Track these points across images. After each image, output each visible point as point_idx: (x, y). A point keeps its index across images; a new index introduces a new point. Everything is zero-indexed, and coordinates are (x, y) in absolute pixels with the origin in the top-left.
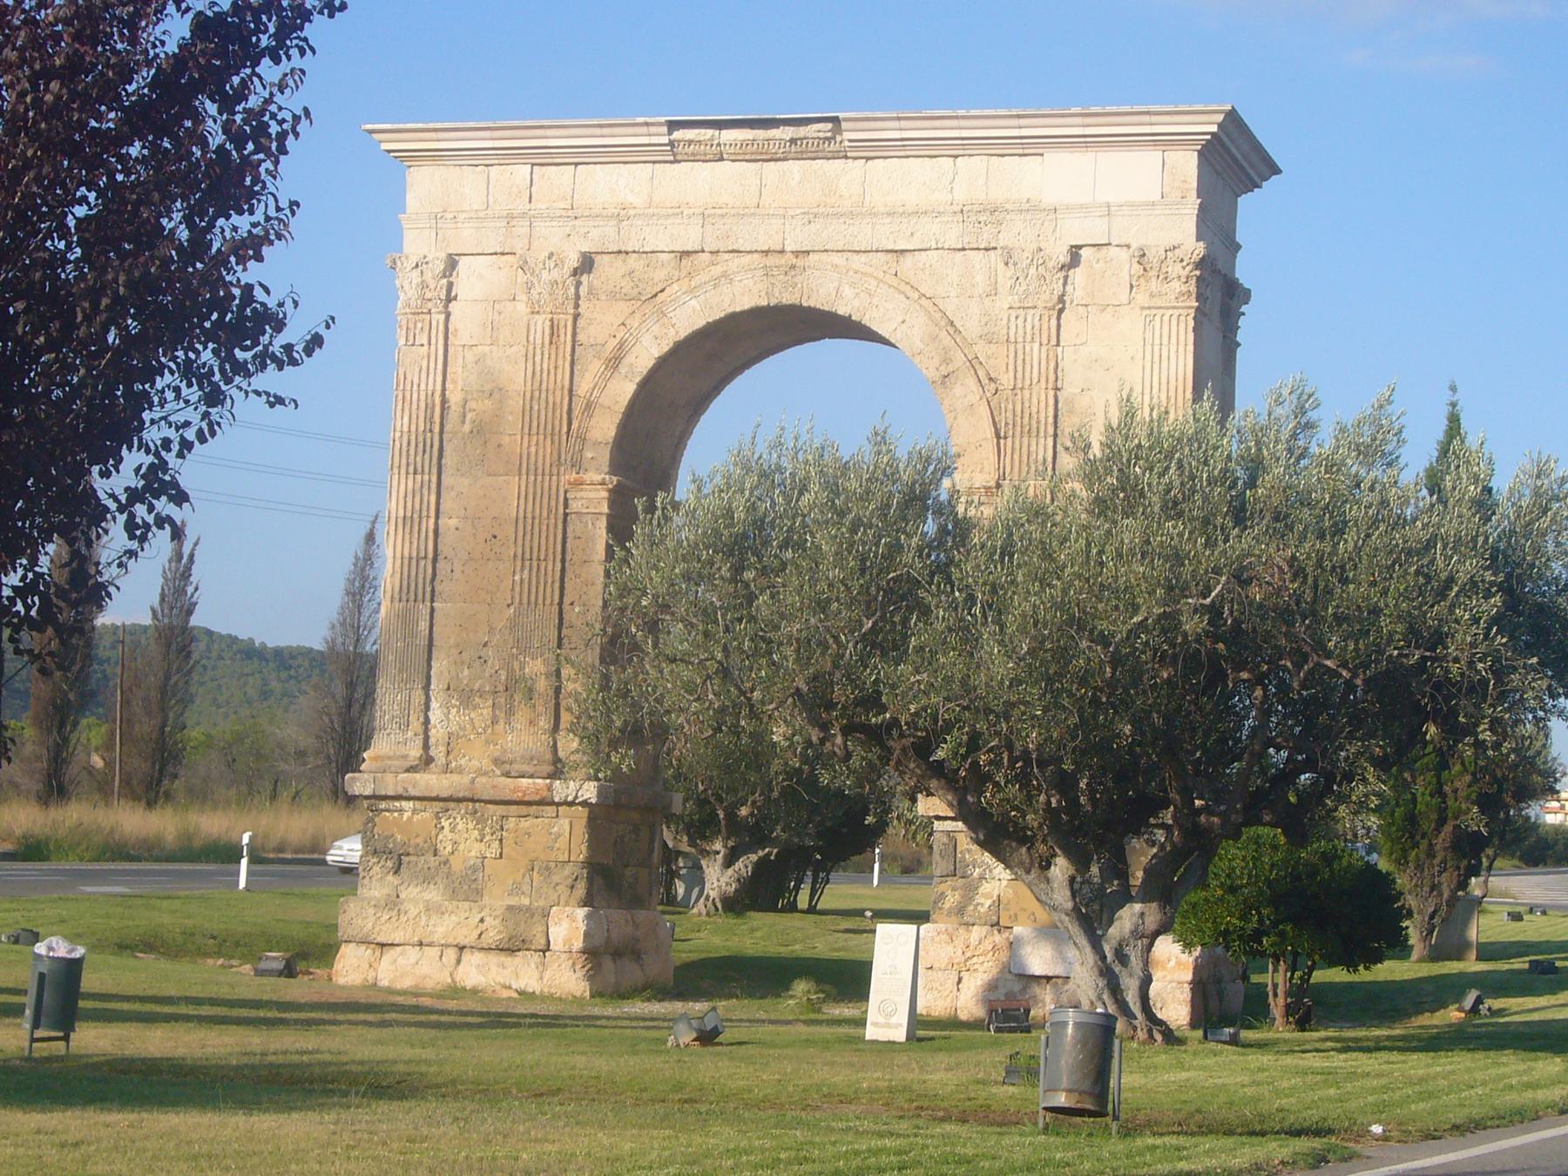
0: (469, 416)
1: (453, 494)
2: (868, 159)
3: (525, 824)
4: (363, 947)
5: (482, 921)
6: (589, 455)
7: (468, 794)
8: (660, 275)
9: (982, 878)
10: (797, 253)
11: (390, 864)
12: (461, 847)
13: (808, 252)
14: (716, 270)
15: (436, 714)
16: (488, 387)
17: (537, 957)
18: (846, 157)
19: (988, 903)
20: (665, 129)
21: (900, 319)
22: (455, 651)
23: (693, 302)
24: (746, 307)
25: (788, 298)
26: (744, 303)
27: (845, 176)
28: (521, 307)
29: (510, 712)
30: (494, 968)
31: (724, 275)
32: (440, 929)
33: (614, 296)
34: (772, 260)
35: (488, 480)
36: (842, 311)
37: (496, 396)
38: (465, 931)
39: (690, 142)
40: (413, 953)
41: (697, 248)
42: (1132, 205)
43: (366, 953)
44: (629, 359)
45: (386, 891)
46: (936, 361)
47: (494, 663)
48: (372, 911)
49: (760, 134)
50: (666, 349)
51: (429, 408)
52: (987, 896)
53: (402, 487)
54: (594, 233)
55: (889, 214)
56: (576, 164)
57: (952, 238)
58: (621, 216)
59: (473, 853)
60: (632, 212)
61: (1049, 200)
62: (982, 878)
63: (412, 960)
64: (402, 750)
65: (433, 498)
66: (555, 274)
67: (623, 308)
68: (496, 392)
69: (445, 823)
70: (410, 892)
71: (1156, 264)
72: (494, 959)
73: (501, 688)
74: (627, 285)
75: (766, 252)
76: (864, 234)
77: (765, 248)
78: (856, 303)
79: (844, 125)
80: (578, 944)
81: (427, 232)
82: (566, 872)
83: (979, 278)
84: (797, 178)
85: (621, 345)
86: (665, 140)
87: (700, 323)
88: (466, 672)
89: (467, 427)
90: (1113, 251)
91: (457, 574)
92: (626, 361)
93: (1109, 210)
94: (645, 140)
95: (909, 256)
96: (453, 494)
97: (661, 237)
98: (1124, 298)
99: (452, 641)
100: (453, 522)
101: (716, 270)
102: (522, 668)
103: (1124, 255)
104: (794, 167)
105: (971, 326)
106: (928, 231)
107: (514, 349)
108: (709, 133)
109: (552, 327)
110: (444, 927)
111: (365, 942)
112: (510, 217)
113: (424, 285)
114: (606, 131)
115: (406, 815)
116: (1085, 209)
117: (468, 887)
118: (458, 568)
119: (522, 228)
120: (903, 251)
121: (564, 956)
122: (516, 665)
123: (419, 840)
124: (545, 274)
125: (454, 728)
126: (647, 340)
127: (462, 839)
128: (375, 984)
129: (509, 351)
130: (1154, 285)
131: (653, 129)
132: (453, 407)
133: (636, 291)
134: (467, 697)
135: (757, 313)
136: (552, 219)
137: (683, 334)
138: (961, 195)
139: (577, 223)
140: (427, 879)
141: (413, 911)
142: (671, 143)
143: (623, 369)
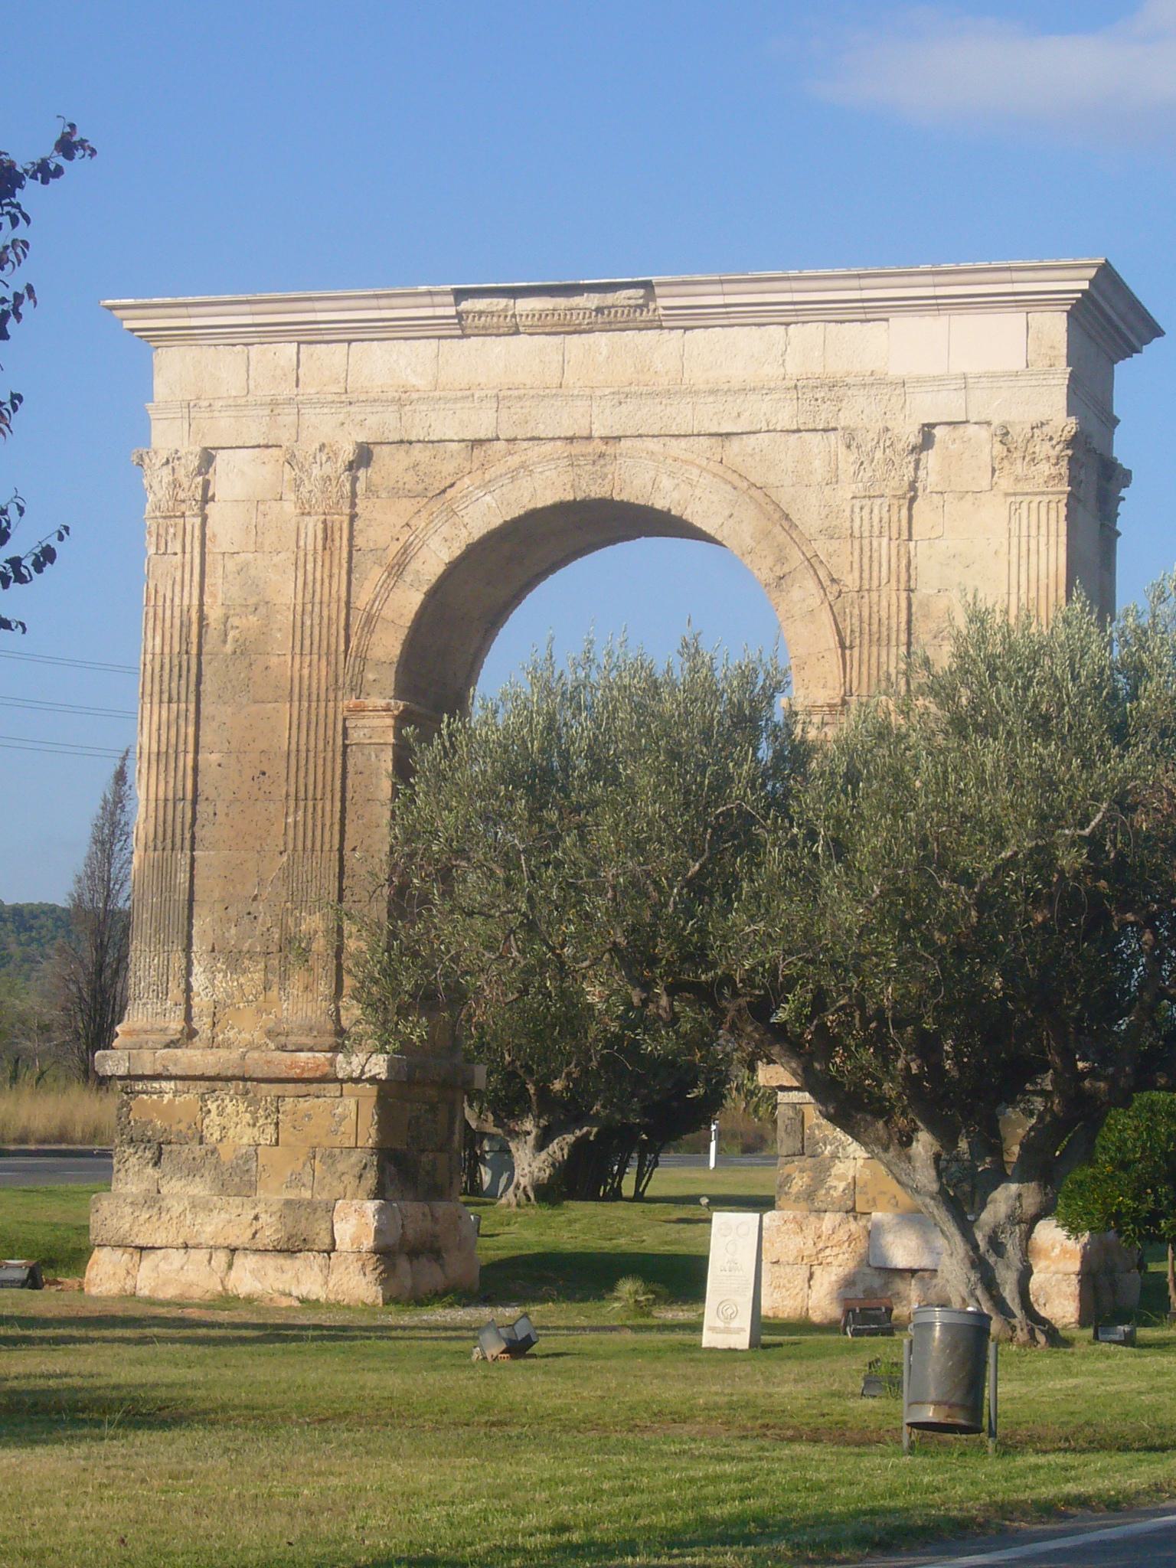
0: (231, 634)
1: (215, 725)
2: (686, 329)
3: (304, 1105)
4: (120, 1252)
5: (256, 1218)
6: (371, 676)
7: (237, 1072)
8: (449, 467)
9: (834, 1156)
10: (606, 440)
11: (148, 1154)
12: (231, 1133)
13: (619, 438)
14: (514, 461)
15: (198, 980)
16: (252, 601)
17: (321, 1259)
18: (661, 328)
19: (842, 1186)
20: (451, 299)
21: (727, 513)
22: (219, 907)
23: (488, 498)
24: (549, 502)
25: (597, 491)
26: (546, 498)
27: (660, 350)
28: (289, 508)
29: (285, 976)
30: (271, 1272)
31: (523, 466)
32: (209, 1229)
33: (396, 493)
34: (578, 448)
36: (660, 504)
37: (262, 610)
38: (237, 1231)
39: (481, 313)
40: (177, 1257)
42: (993, 376)
43: (122, 1258)
44: (414, 566)
45: (145, 1185)
46: (770, 561)
47: (265, 919)
48: (128, 1210)
49: (561, 302)
50: (458, 553)
51: (185, 626)
52: (840, 1178)
53: (155, 718)
54: (372, 420)
55: (713, 392)
56: (350, 342)
57: (785, 418)
58: (402, 399)
59: (245, 1141)
60: (415, 396)
61: (895, 372)
62: (834, 1156)
63: (177, 1265)
64: (160, 1023)
65: (191, 730)
66: (328, 469)
67: (406, 506)
68: (262, 606)
69: (212, 1106)
70: (173, 1187)
72: (271, 1262)
73: (274, 948)
74: (410, 479)
75: (571, 439)
76: (683, 416)
77: (570, 434)
78: (676, 495)
79: (658, 291)
80: (369, 1243)
81: (178, 422)
82: (353, 1160)
83: (817, 463)
84: (605, 352)
85: (405, 549)
86: (452, 311)
87: (497, 522)
88: (233, 931)
89: (229, 648)
90: (971, 429)
91: (221, 818)
94: (429, 312)
95: (735, 440)
96: (215, 725)
97: (448, 425)
98: (985, 484)
99: (216, 895)
100: (215, 757)
101: (514, 461)
102: (298, 925)
103: (984, 433)
104: (602, 341)
105: (809, 516)
107: (282, 556)
108: (502, 302)
109: (325, 530)
110: (211, 1227)
111: (121, 1245)
112: (274, 404)
113: (176, 484)
114: (383, 302)
115: (167, 1098)
116: (939, 381)
117: (238, 1179)
118: (221, 809)
119: (288, 416)
120: (728, 435)
121: (352, 1257)
122: (291, 922)
123: (182, 1126)
124: (316, 471)
125: (220, 996)
126: (435, 543)
127: (232, 1125)
128: (134, 1295)
129: (276, 559)
130: (1019, 468)
131: (437, 300)
132: (213, 625)
133: (421, 487)
134: (233, 959)
135: (561, 509)
136: (323, 405)
137: (477, 535)
138: (793, 369)
139: (353, 409)
140: (192, 1170)
141: (177, 1209)
142: (459, 315)
143: (408, 577)
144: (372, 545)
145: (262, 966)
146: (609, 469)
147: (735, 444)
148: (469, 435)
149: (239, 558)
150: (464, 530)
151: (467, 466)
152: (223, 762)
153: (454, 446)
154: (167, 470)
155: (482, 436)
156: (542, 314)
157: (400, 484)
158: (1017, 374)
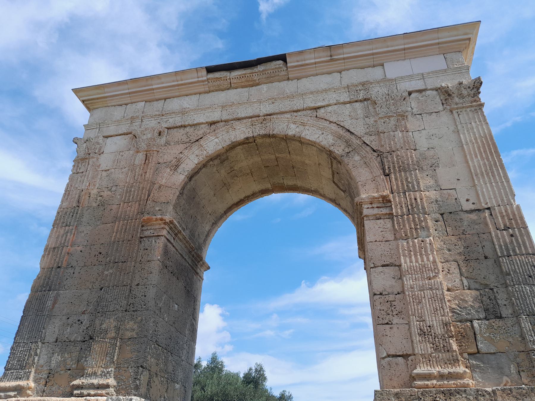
6: (157, 209)
8: (201, 132)
18: (288, 79)
20: (204, 72)
21: (321, 133)
22: (64, 318)
23: (216, 140)
27: (289, 87)
33: (178, 143)
34: (253, 119)
35: (102, 226)
36: (290, 133)
41: (219, 119)
46: (343, 147)
49: (248, 71)
55: (312, 93)
57: (345, 97)
58: (183, 112)
60: (187, 110)
71: (456, 92)
74: (184, 138)
75: (251, 117)
76: (298, 104)
78: (297, 130)
84: (265, 89)
86: (205, 78)
90: (428, 92)
92: (180, 167)
93: (423, 77)
96: (83, 234)
97: (202, 118)
102: (101, 324)
103: (435, 92)
104: (264, 87)
105: (359, 129)
106: (332, 97)
116: (411, 77)
118: (77, 270)
119: (137, 123)
120: (319, 108)
133: (188, 139)
139: (163, 117)
143: (180, 170)
144: (165, 161)
145: (78, 349)
146: (268, 124)
147: (322, 110)
148: (210, 120)
149: (108, 172)
150: (205, 152)
151: (208, 131)
152: (83, 250)
153: (203, 126)
154: (85, 145)
155: (215, 119)
156: (240, 77)
157: (180, 140)
158: (445, 70)
